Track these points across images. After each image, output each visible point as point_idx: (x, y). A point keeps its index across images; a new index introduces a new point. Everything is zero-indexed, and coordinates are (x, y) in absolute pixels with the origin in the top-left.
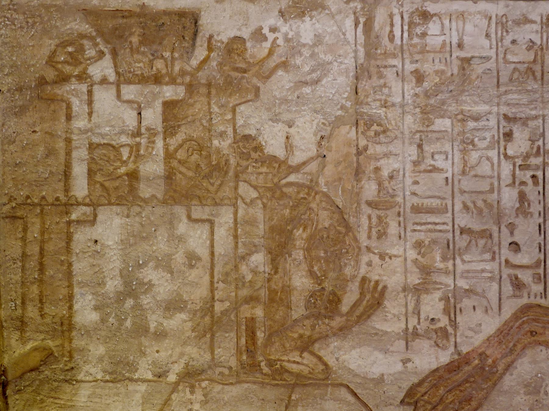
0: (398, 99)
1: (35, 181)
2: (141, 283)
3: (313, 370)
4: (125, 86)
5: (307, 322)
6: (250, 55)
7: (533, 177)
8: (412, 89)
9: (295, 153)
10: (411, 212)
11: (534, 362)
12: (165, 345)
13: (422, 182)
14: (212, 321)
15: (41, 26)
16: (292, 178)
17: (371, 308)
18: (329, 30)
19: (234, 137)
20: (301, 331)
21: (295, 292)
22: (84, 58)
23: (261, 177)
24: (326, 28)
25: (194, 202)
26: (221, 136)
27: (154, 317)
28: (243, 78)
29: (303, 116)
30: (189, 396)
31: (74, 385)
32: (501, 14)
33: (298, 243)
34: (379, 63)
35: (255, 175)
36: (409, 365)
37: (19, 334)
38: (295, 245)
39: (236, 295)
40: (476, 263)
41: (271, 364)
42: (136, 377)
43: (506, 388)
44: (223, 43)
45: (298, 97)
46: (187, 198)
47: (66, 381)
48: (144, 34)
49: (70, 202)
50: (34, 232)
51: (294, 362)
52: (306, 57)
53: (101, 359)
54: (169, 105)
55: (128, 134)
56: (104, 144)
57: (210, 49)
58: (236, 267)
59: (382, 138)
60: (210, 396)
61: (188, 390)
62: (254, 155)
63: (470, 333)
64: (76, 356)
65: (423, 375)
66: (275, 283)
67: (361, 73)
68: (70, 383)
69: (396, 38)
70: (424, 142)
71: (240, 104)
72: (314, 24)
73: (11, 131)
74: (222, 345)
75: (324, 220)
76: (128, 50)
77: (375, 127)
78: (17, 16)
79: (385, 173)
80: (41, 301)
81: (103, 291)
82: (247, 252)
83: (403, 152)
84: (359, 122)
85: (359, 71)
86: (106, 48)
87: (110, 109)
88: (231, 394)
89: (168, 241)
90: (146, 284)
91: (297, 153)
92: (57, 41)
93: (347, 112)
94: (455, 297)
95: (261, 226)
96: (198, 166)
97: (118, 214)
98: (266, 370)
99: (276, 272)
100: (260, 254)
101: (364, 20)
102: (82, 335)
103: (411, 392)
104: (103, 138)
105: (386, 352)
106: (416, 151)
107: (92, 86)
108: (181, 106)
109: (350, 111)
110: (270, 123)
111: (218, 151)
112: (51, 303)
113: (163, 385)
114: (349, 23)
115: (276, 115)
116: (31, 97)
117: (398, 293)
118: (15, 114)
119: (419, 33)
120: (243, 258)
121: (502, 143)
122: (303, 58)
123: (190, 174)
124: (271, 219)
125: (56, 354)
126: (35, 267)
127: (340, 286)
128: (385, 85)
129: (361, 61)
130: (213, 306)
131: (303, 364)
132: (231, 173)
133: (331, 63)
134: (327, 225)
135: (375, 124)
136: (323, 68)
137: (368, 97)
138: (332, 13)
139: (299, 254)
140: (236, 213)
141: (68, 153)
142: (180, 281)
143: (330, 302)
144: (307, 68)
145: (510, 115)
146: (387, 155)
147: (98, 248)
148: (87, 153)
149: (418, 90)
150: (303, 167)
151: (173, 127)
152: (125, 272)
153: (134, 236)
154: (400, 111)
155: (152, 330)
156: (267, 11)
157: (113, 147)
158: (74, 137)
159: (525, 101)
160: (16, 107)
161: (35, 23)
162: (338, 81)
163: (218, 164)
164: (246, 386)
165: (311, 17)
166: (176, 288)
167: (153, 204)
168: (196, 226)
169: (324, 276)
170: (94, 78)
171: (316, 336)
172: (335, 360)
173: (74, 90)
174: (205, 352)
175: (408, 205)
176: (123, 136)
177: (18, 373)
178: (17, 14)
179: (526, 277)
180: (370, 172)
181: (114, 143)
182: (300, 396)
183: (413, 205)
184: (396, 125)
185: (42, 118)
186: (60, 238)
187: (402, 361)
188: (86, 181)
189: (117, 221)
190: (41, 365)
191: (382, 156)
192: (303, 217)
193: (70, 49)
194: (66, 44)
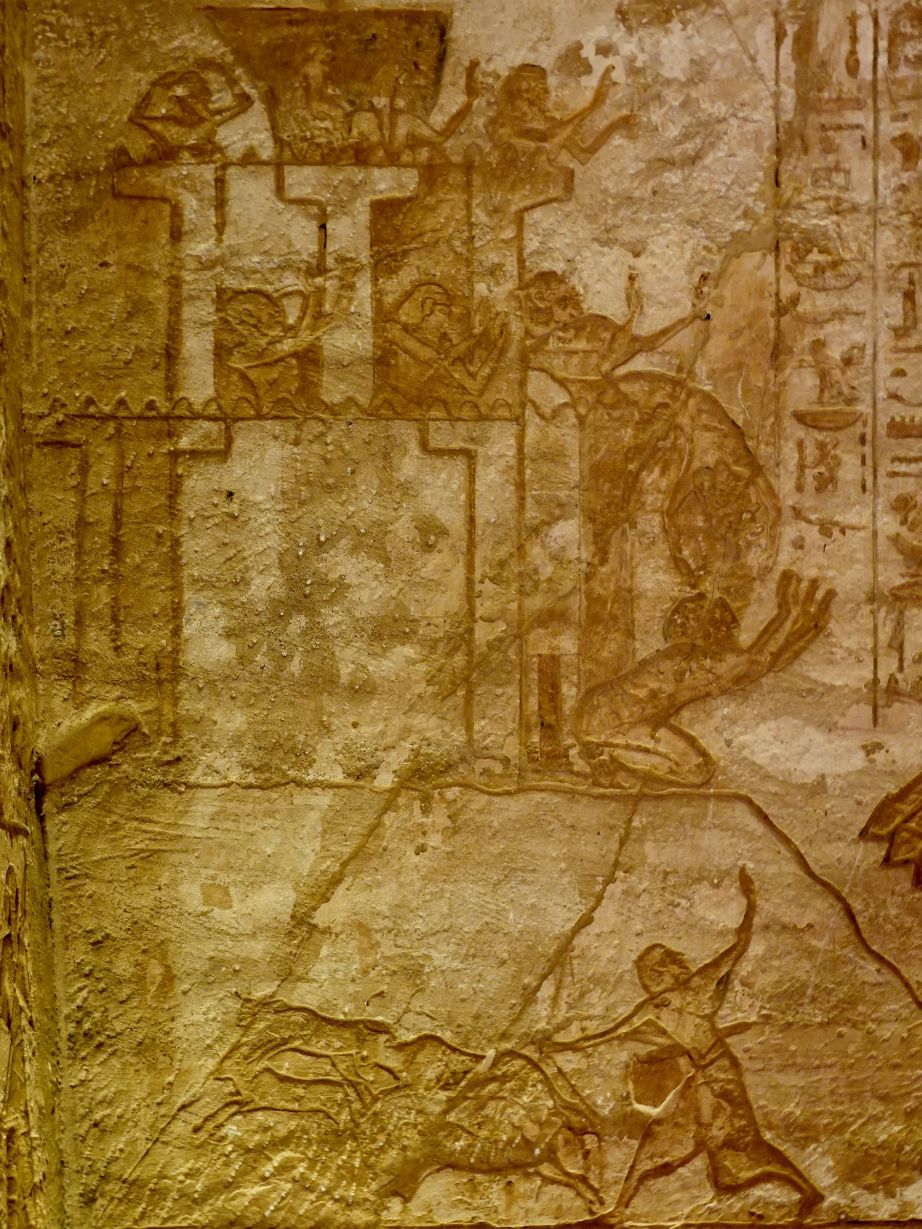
0: (863, 197)
1: (105, 368)
2: (323, 583)
3: (677, 764)
4: (293, 168)
5: (667, 666)
6: (556, 103)
8: (895, 174)
9: (646, 309)
10: (888, 436)
12: (371, 712)
13: (911, 372)
14: (469, 662)
15: (120, 42)
16: (639, 364)
17: (802, 636)
18: (721, 50)
19: (520, 276)
20: (654, 685)
21: (643, 603)
22: (207, 109)
23: (575, 360)
24: (716, 46)
25: (434, 413)
26: (492, 273)
27: (349, 653)
28: (539, 151)
29: (666, 233)
30: (418, 817)
31: (180, 793)
33: (650, 499)
34: (824, 119)
35: (563, 357)
36: (879, 756)
37: (70, 686)
38: (643, 504)
39: (520, 607)
41: (589, 751)
42: (311, 777)
44: (498, 77)
45: (655, 193)
46: (419, 404)
47: (166, 785)
48: (334, 59)
49: (177, 412)
50: (103, 474)
51: (639, 749)
52: (671, 107)
53: (237, 740)
54: (383, 210)
55: (299, 269)
56: (249, 291)
57: (471, 90)
58: (520, 548)
59: (830, 278)
60: (462, 818)
61: (417, 804)
62: (562, 315)
64: (187, 734)
65: (909, 779)
66: (602, 582)
67: (787, 142)
68: (174, 790)
69: (862, 67)
70: (918, 288)
71: (532, 207)
72: (690, 38)
73: (55, 263)
74: (490, 712)
75: (705, 452)
76: (300, 93)
77: (815, 256)
78: (69, 21)
79: (835, 353)
80: (115, 619)
81: (243, 599)
82: (544, 517)
83: (874, 308)
84: (781, 245)
85: (783, 137)
86: (255, 87)
87: (260, 217)
88: (506, 814)
89: (379, 494)
90: (332, 585)
91: (650, 310)
92: (153, 75)
93: (757, 221)
95: (574, 465)
96: (444, 336)
97: (276, 438)
98: (580, 765)
99: (604, 561)
100: (571, 522)
101: (796, 27)
102: (201, 689)
103: (882, 812)
104: (247, 279)
105: (831, 728)
106: (900, 306)
107: (224, 167)
108: (410, 210)
109: (764, 221)
110: (596, 246)
111: (486, 304)
112: (134, 624)
113: (367, 794)
114: (764, 35)
115: (608, 231)
116: (99, 192)
117: (858, 605)
118: (65, 227)
119: (911, 56)
120: (535, 531)
122: (665, 109)
123: (426, 353)
124: (594, 448)
125: (146, 730)
126: (103, 547)
127: (736, 591)
128: (837, 169)
129: (787, 116)
130: (471, 631)
131: (656, 753)
132: (512, 353)
133: (725, 119)
134: (710, 459)
135: (815, 250)
136: (708, 131)
137: (800, 193)
138: (727, 13)
139: (651, 523)
140: (521, 438)
141: (175, 311)
142: (404, 577)
143: (714, 622)
144: (674, 132)
146: (838, 315)
147: (234, 508)
148: (212, 309)
149: (905, 177)
150: (663, 339)
151: (393, 256)
152: (289, 559)
153: (309, 483)
154: (868, 220)
155: (344, 679)
156: (592, 10)
157: (267, 296)
158: (188, 277)
160: (66, 213)
161: (107, 35)
162: (739, 159)
163: (485, 332)
164: (537, 797)
165: (685, 23)
166: (394, 593)
167: (350, 417)
168: (439, 463)
169: (703, 567)
170: (229, 153)
171: (686, 695)
172: (723, 744)
173: (186, 177)
174: (453, 728)
175: (883, 420)
176: (287, 273)
177: (68, 768)
178: (71, 16)
180: (803, 349)
181: (269, 288)
183: (893, 419)
184: (859, 252)
185: (120, 236)
186: (157, 489)
187: (864, 747)
188: (210, 369)
189: (275, 452)
190: (114, 752)
191: (828, 317)
192: (661, 444)
193: (180, 91)
194: (170, 79)
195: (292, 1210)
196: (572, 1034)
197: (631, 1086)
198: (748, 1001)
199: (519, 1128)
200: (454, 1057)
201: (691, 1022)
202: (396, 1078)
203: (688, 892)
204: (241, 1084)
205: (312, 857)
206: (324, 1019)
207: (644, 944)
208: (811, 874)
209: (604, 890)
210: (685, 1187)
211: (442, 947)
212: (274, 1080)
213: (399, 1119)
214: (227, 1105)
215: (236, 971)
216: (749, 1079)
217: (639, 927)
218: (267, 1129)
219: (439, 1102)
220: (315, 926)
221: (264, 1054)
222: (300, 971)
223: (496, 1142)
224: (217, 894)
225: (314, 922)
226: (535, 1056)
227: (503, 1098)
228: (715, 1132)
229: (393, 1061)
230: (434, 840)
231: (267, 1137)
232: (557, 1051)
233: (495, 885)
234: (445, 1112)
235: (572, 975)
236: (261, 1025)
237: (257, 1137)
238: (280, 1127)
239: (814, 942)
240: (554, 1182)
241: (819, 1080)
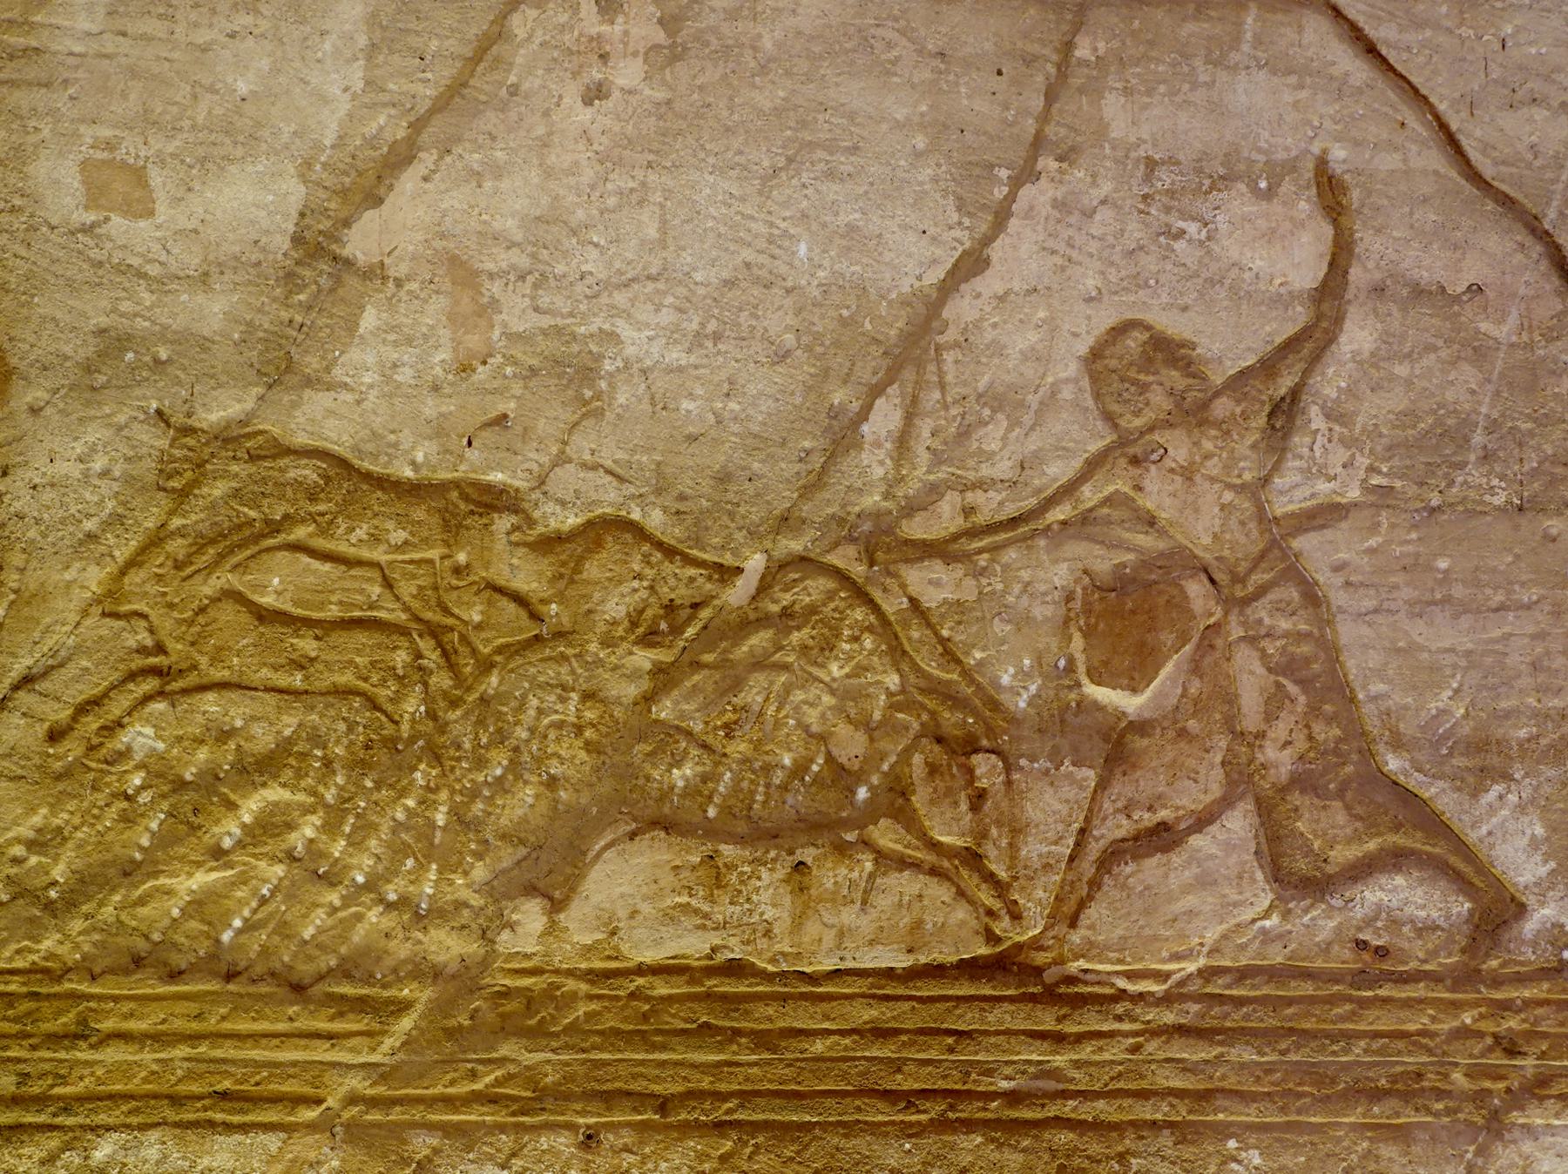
30: (591, 20)
60: (690, 28)
182: (1115, 44)
195: (284, 929)
196: (944, 519)
197: (1078, 643)
198: (1341, 455)
199: (822, 738)
200: (668, 568)
201: (1210, 498)
202: (536, 617)
203: (1204, 208)
204: (166, 624)
205: (344, 106)
206: (367, 476)
207: (1106, 318)
208: (1474, 176)
209: (1011, 198)
210: (1205, 882)
211: (644, 313)
212: (245, 618)
213: (540, 712)
214: (132, 676)
215: (157, 361)
216: (1347, 632)
217: (1091, 283)
218: (225, 735)
219: (634, 676)
220: (349, 263)
221: (221, 557)
222: (312, 363)
223: (767, 769)
224: (118, 184)
225: (346, 252)
226: (858, 570)
227: (786, 667)
228: (1270, 753)
229: (527, 575)
230: (627, 74)
231: (227, 756)
232: (907, 561)
233: (765, 179)
234: (649, 699)
235: (942, 386)
236: (219, 489)
237: (202, 754)
238: (257, 729)
239: (1484, 326)
240: (903, 863)
241: (1507, 637)
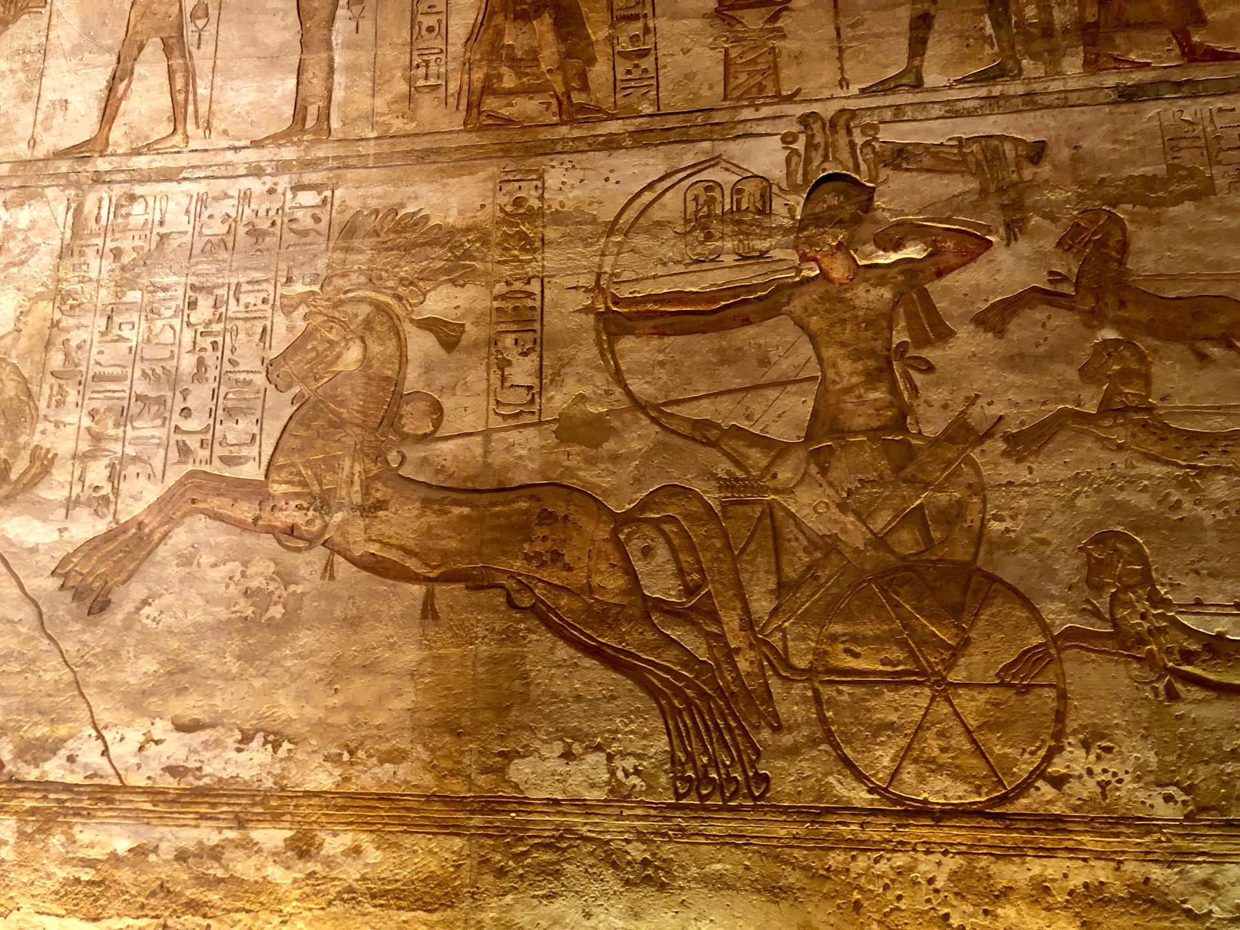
0: (94, 275)
7: (214, 344)
11: (192, 531)
32: (202, 192)
34: (83, 242)
36: (65, 534)
40: (147, 428)
43: (158, 559)
63: (130, 501)
67: (65, 252)
79: (73, 344)
94: (121, 463)
114: (62, 208)
121: (186, 312)
136: (32, 249)
144: (17, 251)
145: (197, 284)
149: (114, 266)
159: (214, 271)
175: (91, 374)
179: (193, 442)
208: (25, 593)
